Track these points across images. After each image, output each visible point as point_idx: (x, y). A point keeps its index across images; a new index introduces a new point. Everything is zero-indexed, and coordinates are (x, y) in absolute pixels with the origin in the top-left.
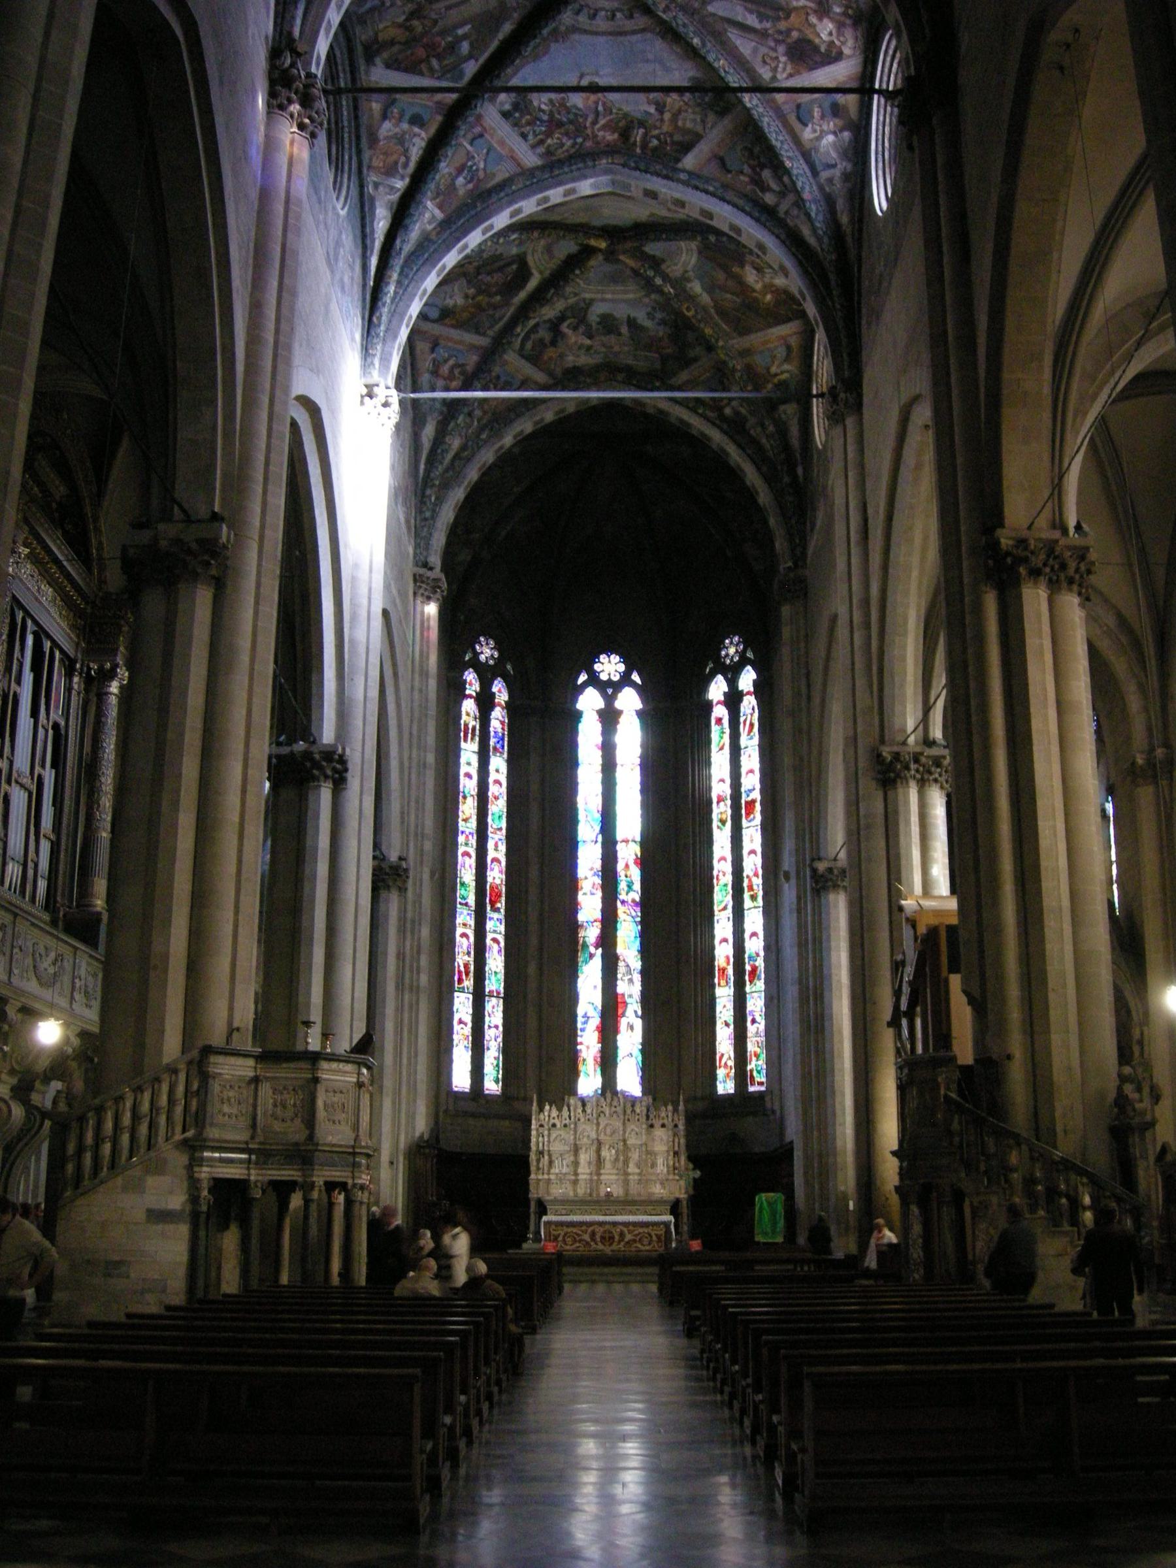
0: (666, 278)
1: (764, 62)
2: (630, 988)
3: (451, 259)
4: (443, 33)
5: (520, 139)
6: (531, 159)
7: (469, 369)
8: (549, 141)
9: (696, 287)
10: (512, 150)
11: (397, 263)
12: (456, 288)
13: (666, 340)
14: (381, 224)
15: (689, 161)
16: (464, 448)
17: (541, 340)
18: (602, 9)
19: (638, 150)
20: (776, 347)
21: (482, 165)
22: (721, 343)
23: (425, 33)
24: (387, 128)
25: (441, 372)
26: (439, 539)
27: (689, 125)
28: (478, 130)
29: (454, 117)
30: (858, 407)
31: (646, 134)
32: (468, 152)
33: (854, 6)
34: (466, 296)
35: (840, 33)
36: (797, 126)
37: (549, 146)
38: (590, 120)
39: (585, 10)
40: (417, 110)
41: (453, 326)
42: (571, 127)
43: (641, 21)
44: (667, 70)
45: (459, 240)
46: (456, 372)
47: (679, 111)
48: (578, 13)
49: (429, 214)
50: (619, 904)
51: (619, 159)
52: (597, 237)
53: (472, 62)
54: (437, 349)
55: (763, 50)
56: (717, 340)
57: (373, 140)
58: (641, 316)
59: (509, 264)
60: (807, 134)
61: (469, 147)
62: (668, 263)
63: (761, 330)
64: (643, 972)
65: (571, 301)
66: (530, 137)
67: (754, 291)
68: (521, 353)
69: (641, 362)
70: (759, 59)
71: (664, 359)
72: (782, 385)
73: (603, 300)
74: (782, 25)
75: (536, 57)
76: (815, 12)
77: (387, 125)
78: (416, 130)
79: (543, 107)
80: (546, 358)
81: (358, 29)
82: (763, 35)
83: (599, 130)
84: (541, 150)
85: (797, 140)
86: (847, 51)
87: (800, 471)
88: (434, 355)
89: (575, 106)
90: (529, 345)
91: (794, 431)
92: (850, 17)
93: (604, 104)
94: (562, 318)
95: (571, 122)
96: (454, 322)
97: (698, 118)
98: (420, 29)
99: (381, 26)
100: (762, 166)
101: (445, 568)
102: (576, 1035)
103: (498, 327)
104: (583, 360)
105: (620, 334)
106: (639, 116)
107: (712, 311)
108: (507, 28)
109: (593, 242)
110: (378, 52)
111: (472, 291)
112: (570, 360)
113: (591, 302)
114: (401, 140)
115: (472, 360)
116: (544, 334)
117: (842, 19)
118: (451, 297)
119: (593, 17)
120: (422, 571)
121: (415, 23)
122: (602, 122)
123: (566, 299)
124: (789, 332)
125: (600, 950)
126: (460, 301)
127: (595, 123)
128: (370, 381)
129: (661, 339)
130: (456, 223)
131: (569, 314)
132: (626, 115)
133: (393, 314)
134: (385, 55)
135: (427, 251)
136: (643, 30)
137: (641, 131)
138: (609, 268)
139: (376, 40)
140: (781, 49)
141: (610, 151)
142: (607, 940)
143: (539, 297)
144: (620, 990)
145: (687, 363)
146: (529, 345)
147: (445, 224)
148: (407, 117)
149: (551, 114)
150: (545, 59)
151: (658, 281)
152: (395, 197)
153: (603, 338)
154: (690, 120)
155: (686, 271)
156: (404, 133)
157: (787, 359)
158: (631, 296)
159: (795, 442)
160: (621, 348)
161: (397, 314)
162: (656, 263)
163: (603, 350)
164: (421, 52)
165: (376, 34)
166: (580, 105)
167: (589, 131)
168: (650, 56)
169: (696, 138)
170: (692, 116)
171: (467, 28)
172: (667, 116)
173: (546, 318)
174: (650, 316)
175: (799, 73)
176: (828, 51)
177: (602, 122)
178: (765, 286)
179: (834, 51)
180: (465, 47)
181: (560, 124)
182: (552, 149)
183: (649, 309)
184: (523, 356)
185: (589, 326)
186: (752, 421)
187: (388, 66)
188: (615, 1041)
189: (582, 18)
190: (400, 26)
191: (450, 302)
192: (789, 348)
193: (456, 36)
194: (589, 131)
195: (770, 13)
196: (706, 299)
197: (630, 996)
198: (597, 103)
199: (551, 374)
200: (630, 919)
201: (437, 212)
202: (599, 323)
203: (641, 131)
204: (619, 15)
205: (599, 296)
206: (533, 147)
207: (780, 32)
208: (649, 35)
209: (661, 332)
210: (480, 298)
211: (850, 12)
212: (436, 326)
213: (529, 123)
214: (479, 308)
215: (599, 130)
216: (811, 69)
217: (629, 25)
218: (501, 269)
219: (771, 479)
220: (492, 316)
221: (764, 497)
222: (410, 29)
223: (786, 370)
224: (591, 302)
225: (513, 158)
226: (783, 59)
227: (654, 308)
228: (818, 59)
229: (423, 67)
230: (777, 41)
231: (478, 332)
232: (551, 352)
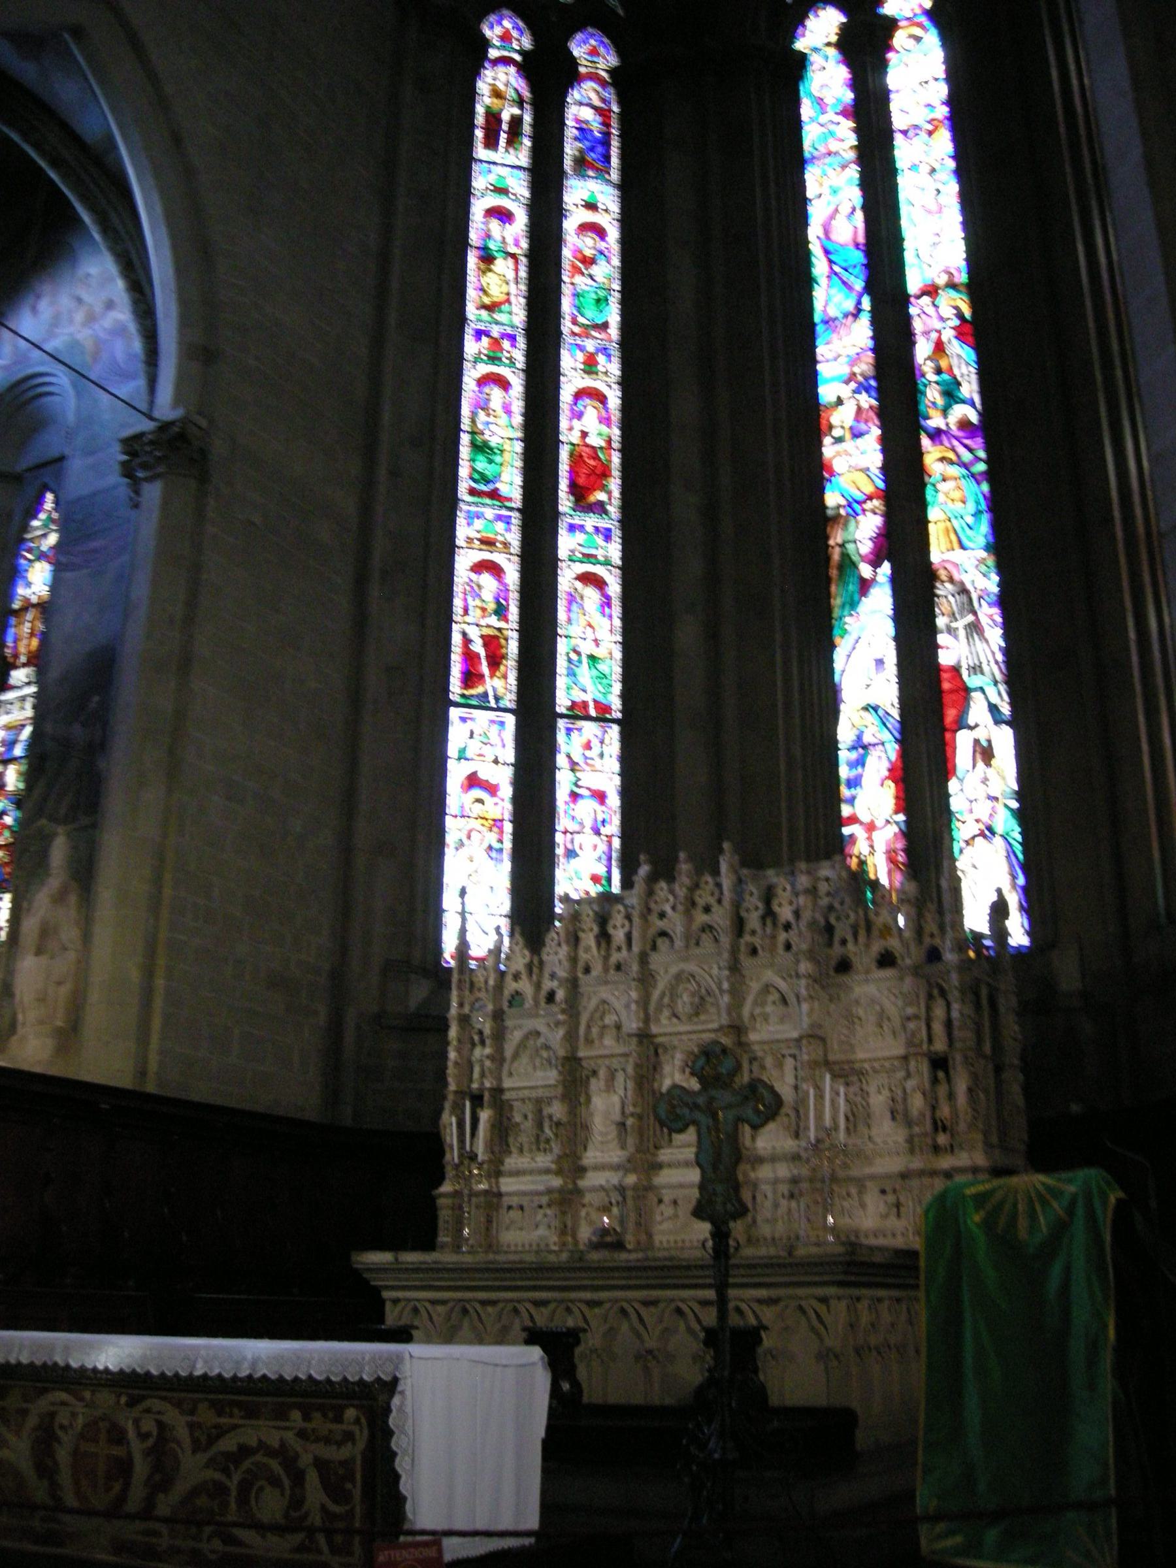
2: (973, 648)
50: (925, 442)
64: (1004, 601)
102: (834, 799)
125: (886, 568)
142: (904, 539)
144: (945, 658)
188: (944, 796)
197: (976, 669)
200: (955, 471)
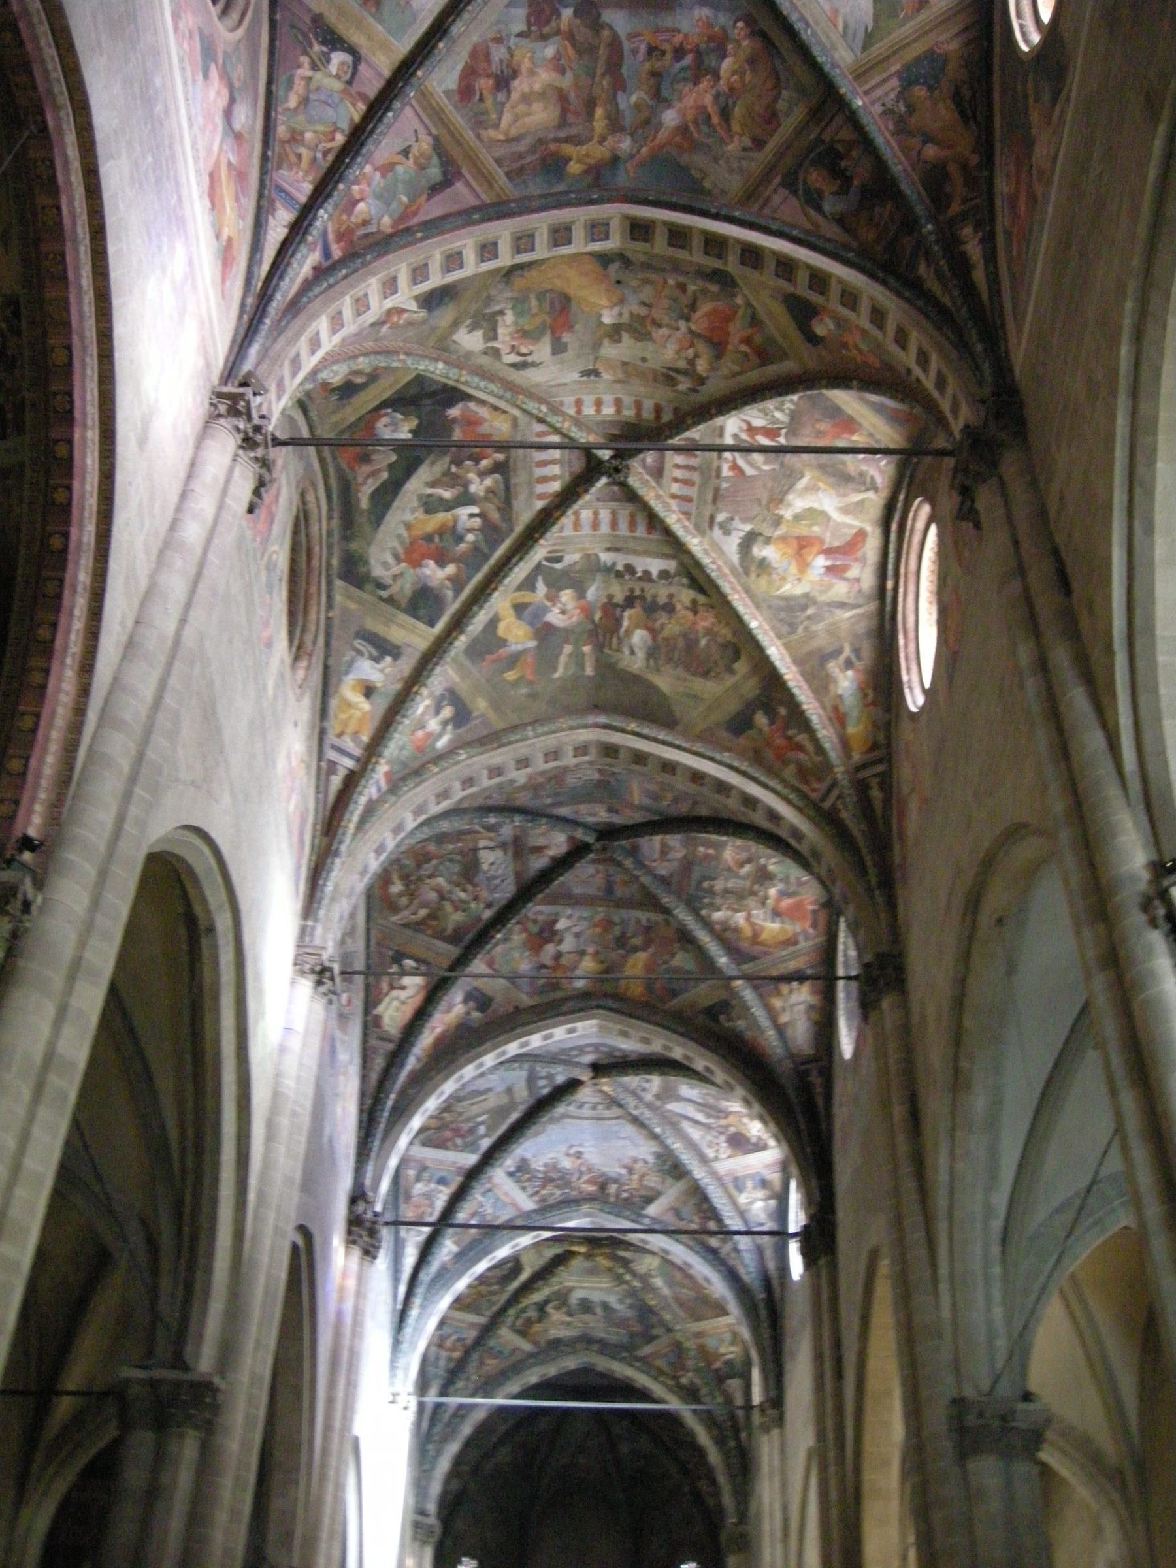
0: (634, 1274)
3: (462, 1284)
4: (468, 1120)
6: (528, 1204)
7: (469, 1342)
8: (544, 1192)
9: (658, 1282)
11: (420, 1291)
15: (652, 1210)
24: (419, 1188)
26: (435, 1488)
28: (488, 1186)
29: (473, 1175)
30: (780, 1421)
36: (735, 1193)
38: (576, 1176)
43: (616, 1111)
45: (468, 1269)
49: (448, 1247)
51: (597, 1205)
52: (579, 1244)
55: (709, 1138)
57: (408, 1197)
58: (612, 1300)
60: (743, 1199)
69: (615, 1335)
71: (632, 1335)
72: (729, 1363)
74: (723, 1122)
75: (537, 1134)
78: (441, 1188)
82: (708, 1127)
84: (537, 1198)
85: (734, 1203)
94: (546, 1302)
100: (709, 1219)
101: (439, 1515)
103: (495, 1308)
108: (515, 1116)
109: (575, 1248)
112: (555, 1333)
113: (571, 1290)
114: (428, 1196)
115: (472, 1335)
116: (532, 1313)
120: (420, 1518)
122: (585, 1178)
128: (395, 1390)
129: (628, 1319)
130: (465, 1257)
132: (603, 1175)
133: (415, 1329)
135: (445, 1277)
136: (617, 1118)
138: (588, 1264)
140: (723, 1138)
141: (591, 1198)
143: (528, 1287)
145: (650, 1339)
146: (519, 1322)
147: (459, 1256)
151: (628, 1277)
152: (422, 1238)
154: (653, 1181)
160: (596, 1326)
161: (418, 1330)
162: (625, 1263)
172: (635, 1177)
174: (621, 1301)
180: (482, 1130)
181: (552, 1180)
186: (703, 1391)
187: (424, 1144)
196: (666, 1291)
199: (535, 1343)
209: (630, 1314)
213: (529, 1180)
217: (608, 1113)
219: (720, 1442)
221: (714, 1456)
222: (442, 1119)
224: (571, 1290)
225: (515, 1205)
229: (449, 1144)
232: (537, 1327)
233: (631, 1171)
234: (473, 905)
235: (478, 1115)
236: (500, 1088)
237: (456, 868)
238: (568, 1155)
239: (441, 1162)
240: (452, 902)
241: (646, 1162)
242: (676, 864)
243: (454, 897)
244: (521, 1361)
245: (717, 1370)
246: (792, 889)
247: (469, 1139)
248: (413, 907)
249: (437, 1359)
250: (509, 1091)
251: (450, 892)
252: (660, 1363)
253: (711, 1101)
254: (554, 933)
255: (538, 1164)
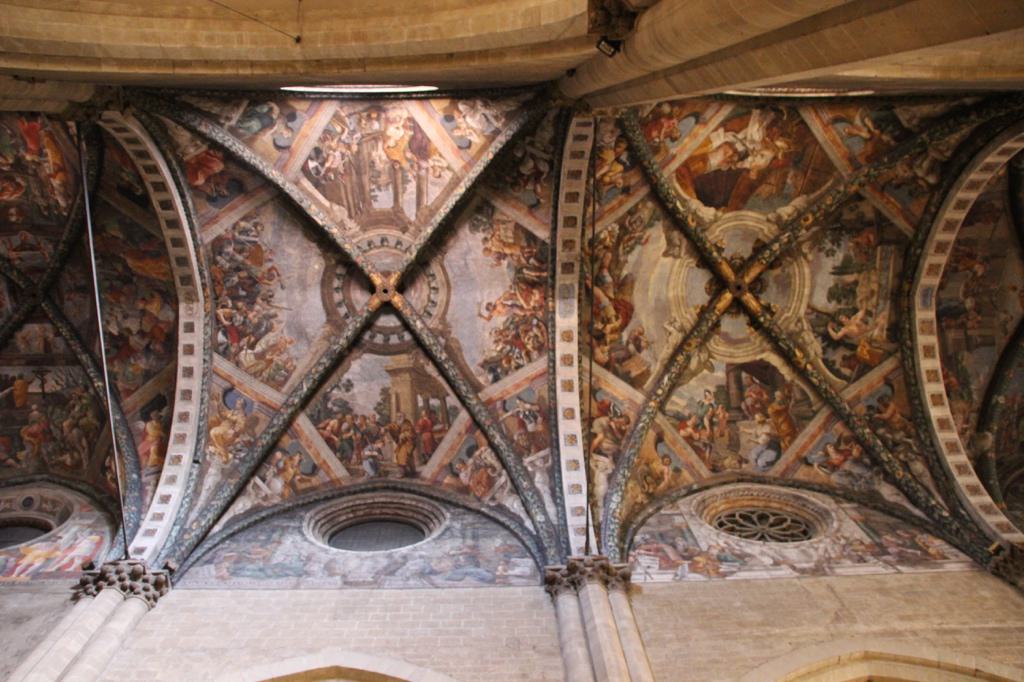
1: (440, 176)
5: (520, 371)
9: (786, 211)
10: (527, 379)
12: (747, 430)
13: (859, 240)
14: (515, 505)
15: (543, 234)
16: (926, 462)
17: (844, 358)
18: (429, 297)
19: (545, 274)
20: (838, 133)
21: (528, 406)
22: (842, 188)
23: (413, 431)
25: (836, 462)
27: (510, 234)
31: (527, 268)
32: (512, 415)
33: (365, 114)
34: (763, 423)
35: (393, 122)
37: (533, 348)
38: (518, 312)
39: (429, 309)
40: (464, 450)
41: (790, 442)
42: (521, 327)
44: (469, 250)
46: (843, 447)
47: (501, 241)
48: (430, 315)
53: (448, 399)
54: (810, 461)
55: (431, 177)
56: (839, 192)
59: (739, 381)
61: (509, 414)
62: (760, 236)
63: (821, 149)
65: (806, 326)
66: (521, 362)
67: (775, 158)
68: (849, 380)
70: (439, 180)
71: (882, 242)
72: (877, 123)
73: (811, 295)
74: (406, 165)
76: (384, 142)
77: (462, 476)
78: (477, 453)
79: (499, 349)
80: (868, 357)
81: (391, 478)
82: (419, 178)
83: (528, 304)
84: (535, 354)
86: (405, 115)
87: (968, 101)
88: (816, 465)
89: (504, 323)
90: (846, 371)
91: (926, 109)
92: (379, 116)
93: (507, 300)
95: (517, 327)
96: (788, 438)
97: (502, 226)
98: (408, 434)
99: (395, 461)
104: (882, 320)
105: (856, 283)
106: (512, 274)
107: (812, 196)
110: (413, 467)
111: (758, 417)
112: (878, 330)
113: (811, 309)
116: (837, 356)
117: (382, 121)
118: (757, 437)
119: (434, 304)
121: (402, 436)
122: (522, 302)
123: (802, 330)
124: (817, 122)
126: (767, 429)
127: (521, 308)
131: (822, 329)
134: (417, 463)
137: (525, 271)
139: (404, 467)
140: (424, 164)
146: (846, 371)
148: (465, 457)
149: (506, 343)
150: (461, 341)
153: (858, 299)
154: (508, 234)
155: (768, 220)
156: (475, 463)
157: (849, 121)
158: (807, 270)
159: (938, 108)
160: (873, 284)
163: (874, 300)
164: (426, 436)
165: (400, 466)
166: (504, 319)
167: (528, 313)
168: (462, 262)
169: (518, 227)
170: (502, 231)
171: (420, 399)
172: (507, 251)
173: (820, 351)
174: (830, 253)
175: (436, 149)
176: (410, 128)
177: (522, 302)
178: (767, 148)
179: (408, 124)
180: (435, 402)
181: (517, 336)
182: (537, 345)
183: (822, 254)
184: (855, 381)
185: (840, 312)
187: (425, 463)
189: (435, 311)
190: (400, 447)
191: (762, 439)
192: (836, 120)
193: (423, 408)
194: (528, 313)
195: (400, 175)
196: (799, 202)
198: (504, 305)
199: (889, 354)
201: (542, 453)
202: (839, 302)
203: (525, 271)
204: (433, 285)
205: (805, 301)
206: (530, 360)
207: (412, 166)
208: (445, 263)
210: (770, 411)
211: (374, 115)
212: (783, 457)
213: (509, 362)
214: (778, 413)
215: (528, 304)
216: (429, 140)
217: (440, 276)
218: (741, 388)
220: (797, 402)
222: (405, 441)
223: (862, 124)
224: (811, 309)
226: (431, 163)
227: (820, 250)
228: (419, 136)
229: (436, 436)
230: (420, 168)
231: (810, 419)
232: (863, 351)
233: (501, 256)
234: (84, 401)
235: (415, 403)
236: (387, 381)
237: (58, 411)
238: (489, 318)
239: (452, 448)
240: (81, 417)
241: (485, 240)
242: (39, 238)
243: (77, 415)
244: (906, 376)
245: (896, 139)
246: (20, 141)
247: (440, 416)
248: (80, 448)
249: (849, 474)
250: (393, 372)
251: (73, 418)
252: (917, 209)
253: (384, 179)
254: (121, 335)
255: (493, 349)
